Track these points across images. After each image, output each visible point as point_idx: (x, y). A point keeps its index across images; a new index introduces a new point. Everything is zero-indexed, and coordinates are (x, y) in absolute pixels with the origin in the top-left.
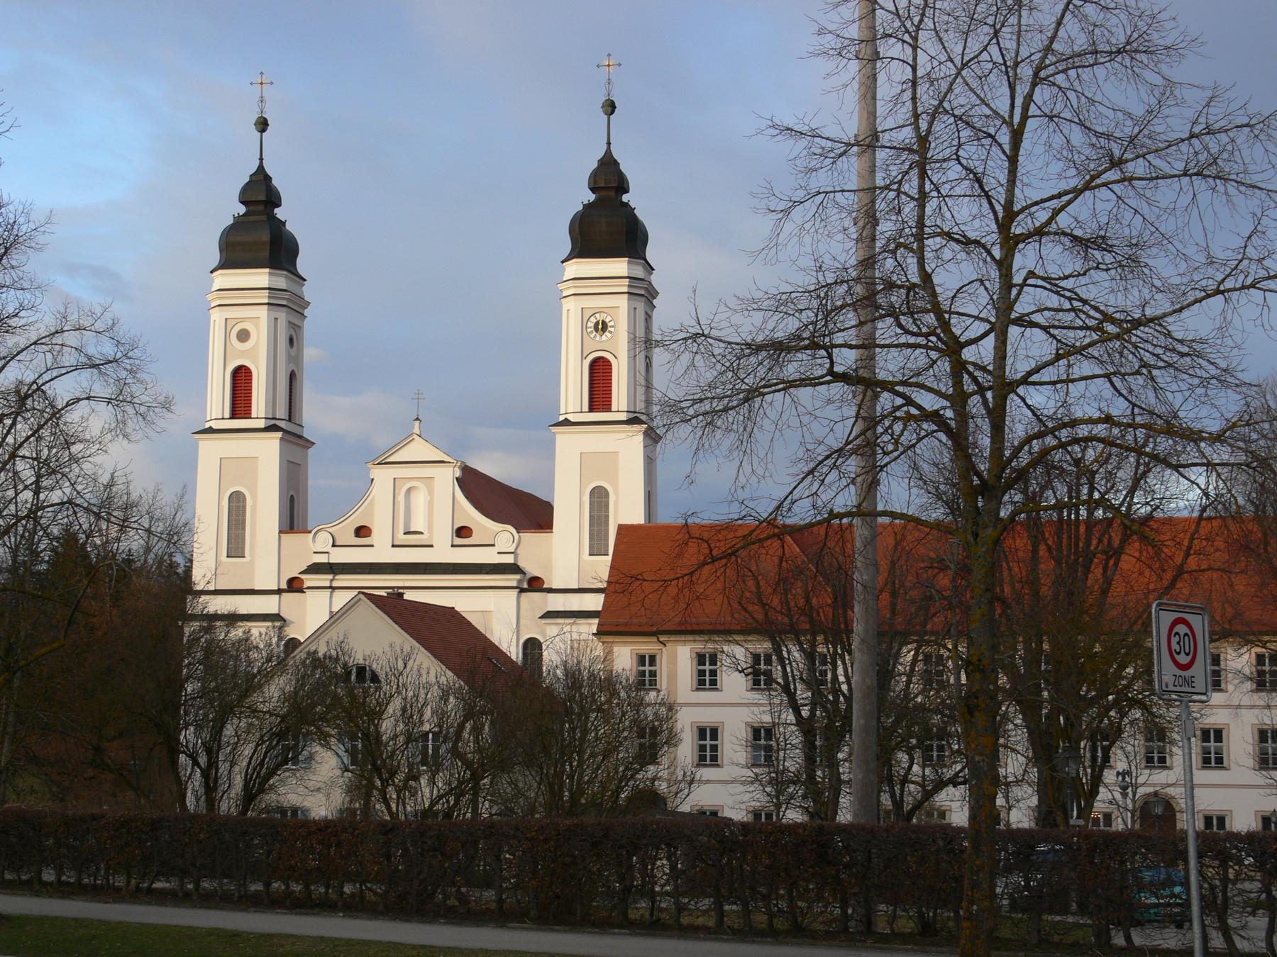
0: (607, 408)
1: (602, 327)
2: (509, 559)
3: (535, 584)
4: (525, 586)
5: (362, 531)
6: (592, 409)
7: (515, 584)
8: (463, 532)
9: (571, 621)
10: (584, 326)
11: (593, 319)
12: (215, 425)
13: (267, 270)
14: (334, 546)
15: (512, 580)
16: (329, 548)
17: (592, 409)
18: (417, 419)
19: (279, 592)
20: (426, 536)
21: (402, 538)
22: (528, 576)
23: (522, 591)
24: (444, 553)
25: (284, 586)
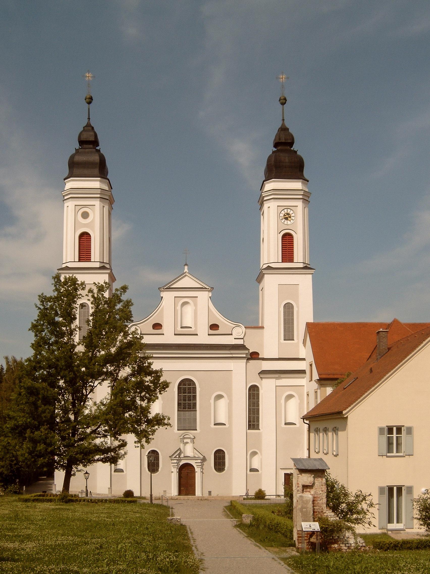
0: (291, 260)
1: (287, 217)
2: (240, 342)
3: (254, 356)
5: (157, 326)
6: (283, 261)
7: (245, 356)
8: (214, 327)
9: (277, 376)
10: (279, 216)
11: (283, 212)
12: (70, 265)
13: (99, 179)
17: (283, 261)
18: (186, 265)
21: (179, 330)
22: (251, 351)
23: (248, 359)
24: (204, 338)
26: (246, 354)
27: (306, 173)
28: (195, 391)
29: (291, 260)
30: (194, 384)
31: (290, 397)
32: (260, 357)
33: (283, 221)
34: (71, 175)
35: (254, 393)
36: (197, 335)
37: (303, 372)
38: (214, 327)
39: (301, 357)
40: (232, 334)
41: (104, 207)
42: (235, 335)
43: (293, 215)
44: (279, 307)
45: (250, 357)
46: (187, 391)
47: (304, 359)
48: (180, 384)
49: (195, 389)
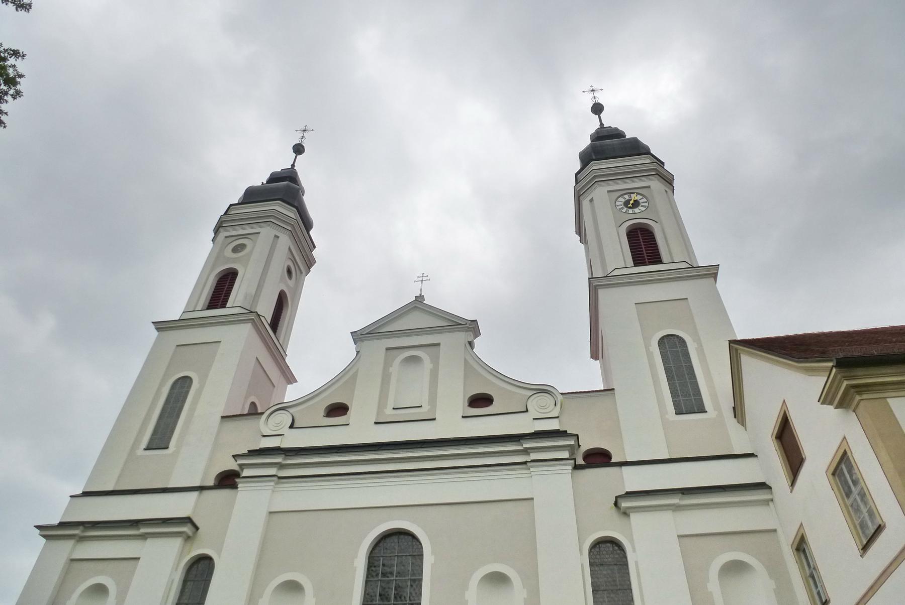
0: (656, 259)
2: (553, 425)
3: (599, 458)
4: (580, 461)
5: (338, 410)
7: (566, 454)
8: (480, 401)
14: (291, 427)
16: (286, 430)
19: (201, 489)
20: (426, 407)
21: (389, 414)
23: (576, 467)
25: (211, 483)
29: (657, 260)
31: (735, 568)
32: (613, 460)
33: (624, 210)
36: (434, 419)
40: (527, 411)
41: (277, 237)
43: (644, 200)
44: (647, 347)
45: (583, 463)
49: (419, 556)
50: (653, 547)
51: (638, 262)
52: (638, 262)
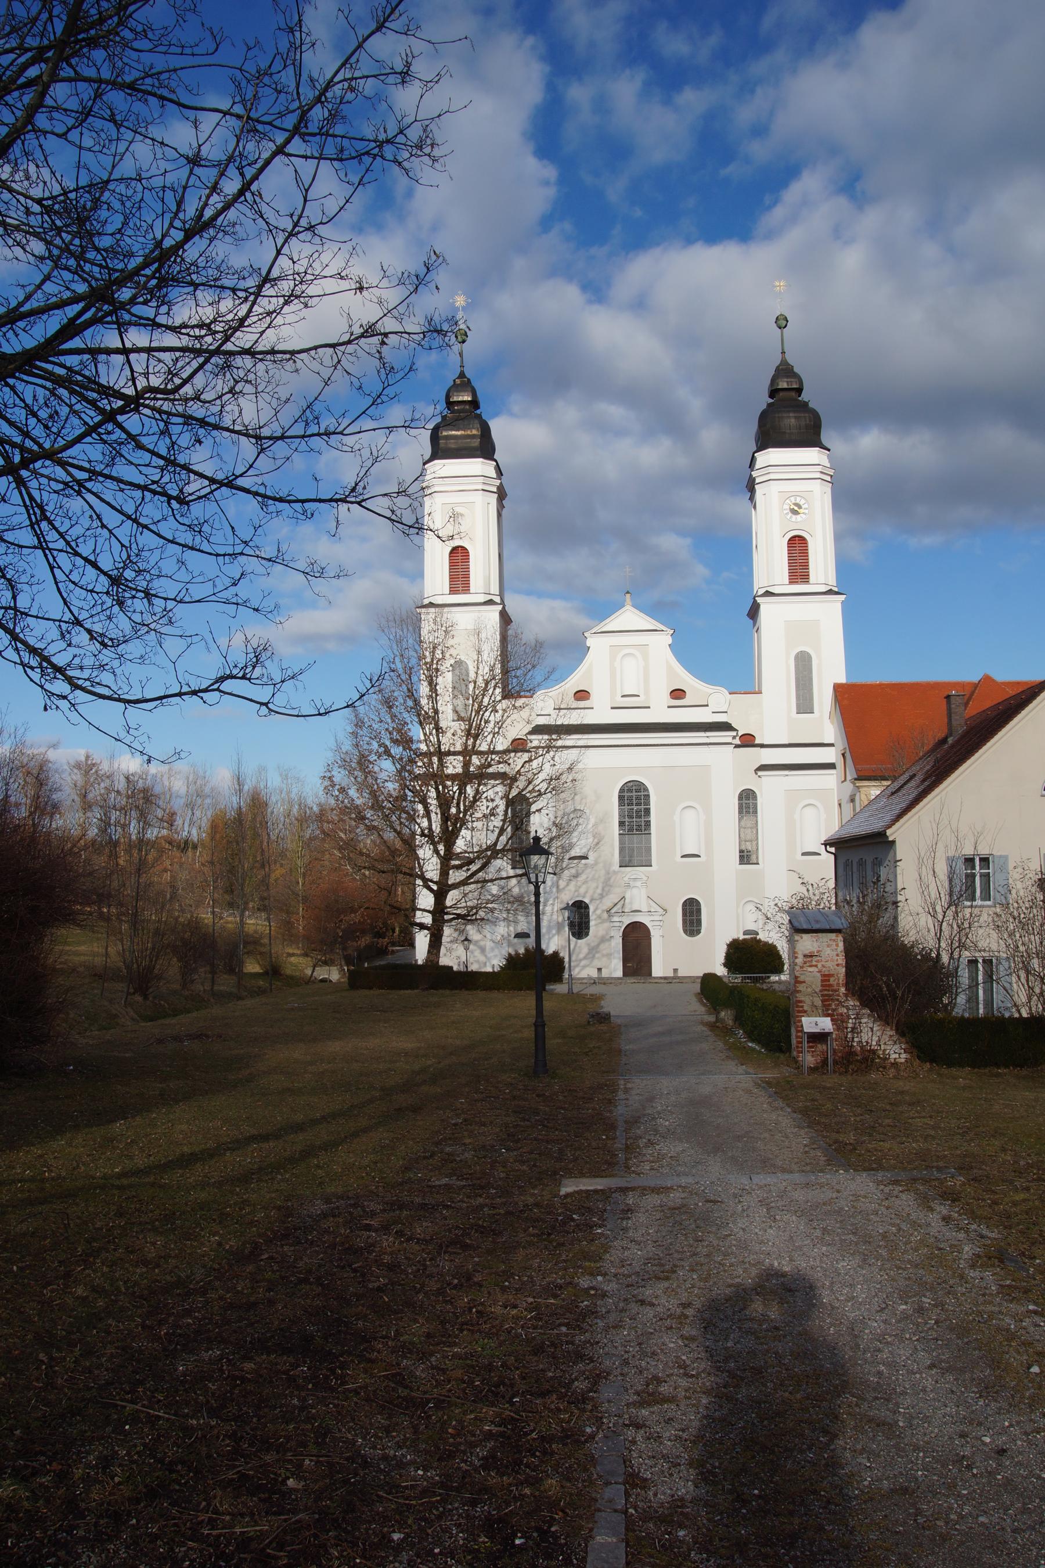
3: (748, 741)
4: (737, 741)
5: (582, 695)
6: (791, 583)
7: (730, 740)
8: (678, 694)
13: (481, 460)
15: (725, 736)
17: (791, 583)
24: (662, 712)
26: (734, 737)
27: (825, 439)
28: (648, 803)
30: (646, 789)
32: (757, 742)
34: (434, 456)
35: (747, 801)
37: (831, 766)
38: (678, 694)
39: (826, 742)
42: (713, 707)
46: (634, 801)
47: (832, 745)
48: (622, 790)
49: (647, 797)
50: (772, 790)
51: (793, 581)
52: (793, 581)
